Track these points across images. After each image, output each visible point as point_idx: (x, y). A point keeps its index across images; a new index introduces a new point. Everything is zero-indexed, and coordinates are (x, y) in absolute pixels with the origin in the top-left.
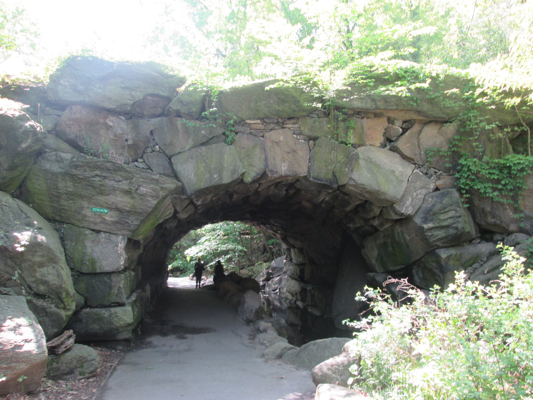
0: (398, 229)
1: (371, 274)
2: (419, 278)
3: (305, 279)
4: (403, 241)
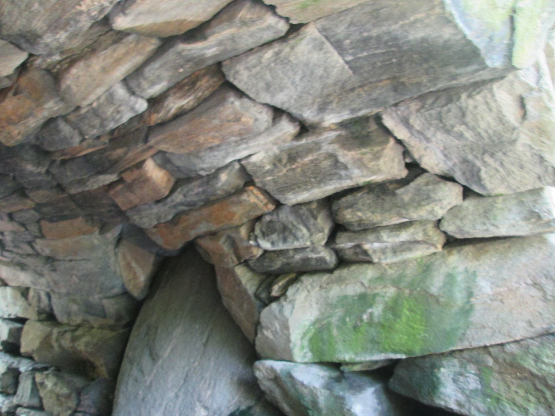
0: (457, 262)
1: (278, 366)
2: (463, 391)
3: (23, 350)
4: (459, 296)
